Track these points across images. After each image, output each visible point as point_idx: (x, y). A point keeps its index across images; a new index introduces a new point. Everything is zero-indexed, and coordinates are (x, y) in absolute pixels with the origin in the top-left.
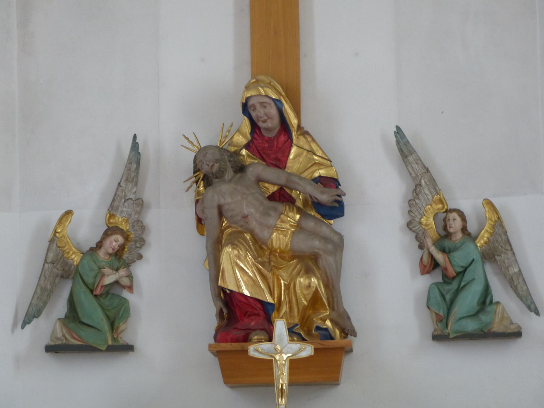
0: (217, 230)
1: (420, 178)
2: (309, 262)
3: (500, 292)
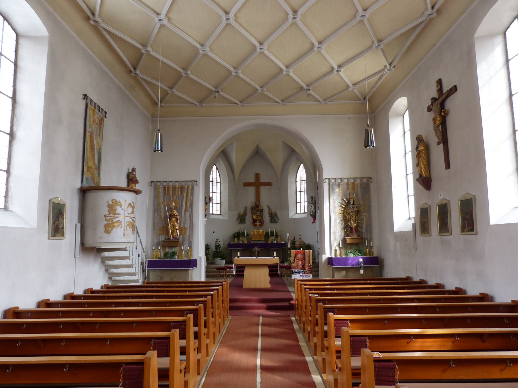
1: (270, 209)
2: (260, 216)
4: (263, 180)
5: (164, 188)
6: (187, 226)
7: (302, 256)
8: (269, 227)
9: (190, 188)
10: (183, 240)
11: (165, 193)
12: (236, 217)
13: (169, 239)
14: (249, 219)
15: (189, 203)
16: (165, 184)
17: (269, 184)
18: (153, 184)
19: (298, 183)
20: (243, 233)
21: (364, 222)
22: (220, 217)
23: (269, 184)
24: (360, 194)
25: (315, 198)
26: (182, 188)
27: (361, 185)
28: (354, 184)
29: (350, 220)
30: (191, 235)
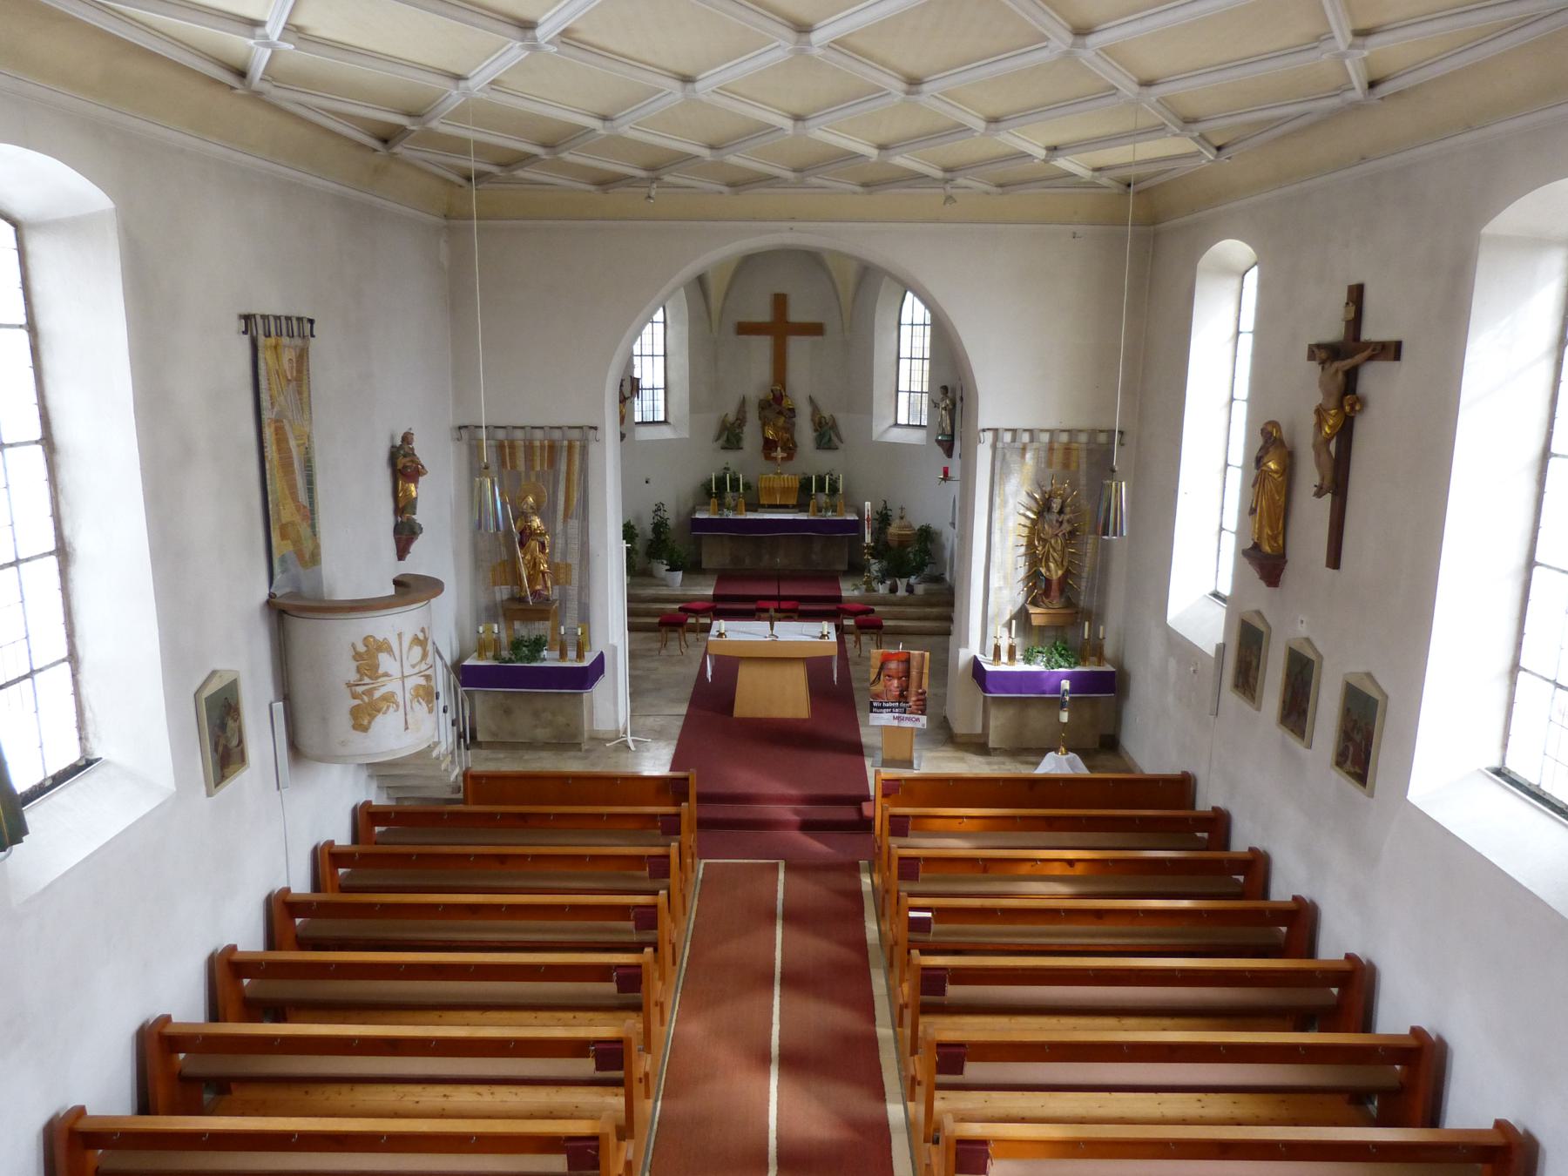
0: (764, 422)
1: (815, 409)
3: (834, 438)
4: (796, 315)
5: (500, 447)
6: (574, 560)
7: (902, 667)
8: (810, 459)
9: (577, 451)
10: (564, 599)
11: (503, 464)
12: (713, 430)
13: (522, 600)
14: (752, 436)
15: (575, 496)
16: (501, 434)
17: (815, 329)
18: (463, 431)
19: (905, 330)
20: (735, 481)
21: (1088, 561)
22: (665, 433)
23: (815, 329)
24: (1083, 481)
25: (954, 391)
26: (553, 448)
27: (1090, 452)
28: (1067, 450)
29: (1047, 560)
30: (585, 587)
